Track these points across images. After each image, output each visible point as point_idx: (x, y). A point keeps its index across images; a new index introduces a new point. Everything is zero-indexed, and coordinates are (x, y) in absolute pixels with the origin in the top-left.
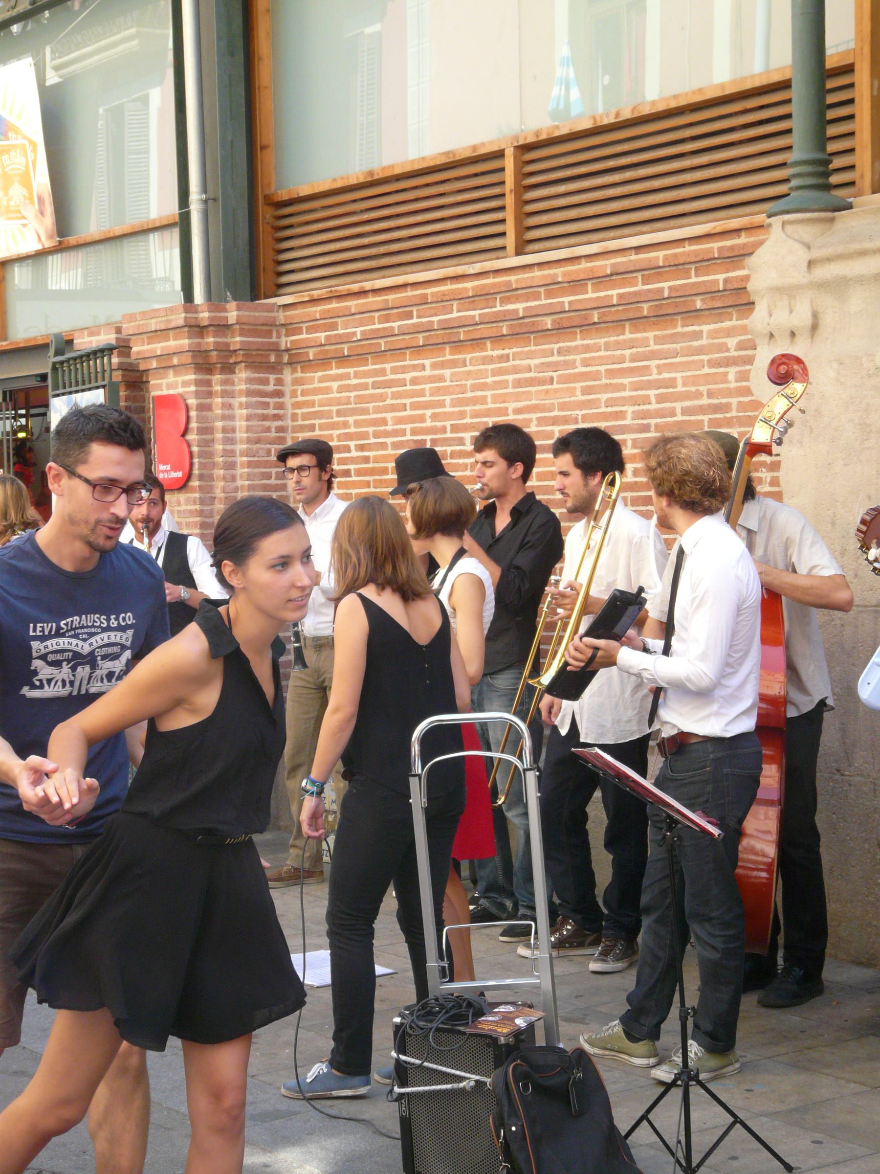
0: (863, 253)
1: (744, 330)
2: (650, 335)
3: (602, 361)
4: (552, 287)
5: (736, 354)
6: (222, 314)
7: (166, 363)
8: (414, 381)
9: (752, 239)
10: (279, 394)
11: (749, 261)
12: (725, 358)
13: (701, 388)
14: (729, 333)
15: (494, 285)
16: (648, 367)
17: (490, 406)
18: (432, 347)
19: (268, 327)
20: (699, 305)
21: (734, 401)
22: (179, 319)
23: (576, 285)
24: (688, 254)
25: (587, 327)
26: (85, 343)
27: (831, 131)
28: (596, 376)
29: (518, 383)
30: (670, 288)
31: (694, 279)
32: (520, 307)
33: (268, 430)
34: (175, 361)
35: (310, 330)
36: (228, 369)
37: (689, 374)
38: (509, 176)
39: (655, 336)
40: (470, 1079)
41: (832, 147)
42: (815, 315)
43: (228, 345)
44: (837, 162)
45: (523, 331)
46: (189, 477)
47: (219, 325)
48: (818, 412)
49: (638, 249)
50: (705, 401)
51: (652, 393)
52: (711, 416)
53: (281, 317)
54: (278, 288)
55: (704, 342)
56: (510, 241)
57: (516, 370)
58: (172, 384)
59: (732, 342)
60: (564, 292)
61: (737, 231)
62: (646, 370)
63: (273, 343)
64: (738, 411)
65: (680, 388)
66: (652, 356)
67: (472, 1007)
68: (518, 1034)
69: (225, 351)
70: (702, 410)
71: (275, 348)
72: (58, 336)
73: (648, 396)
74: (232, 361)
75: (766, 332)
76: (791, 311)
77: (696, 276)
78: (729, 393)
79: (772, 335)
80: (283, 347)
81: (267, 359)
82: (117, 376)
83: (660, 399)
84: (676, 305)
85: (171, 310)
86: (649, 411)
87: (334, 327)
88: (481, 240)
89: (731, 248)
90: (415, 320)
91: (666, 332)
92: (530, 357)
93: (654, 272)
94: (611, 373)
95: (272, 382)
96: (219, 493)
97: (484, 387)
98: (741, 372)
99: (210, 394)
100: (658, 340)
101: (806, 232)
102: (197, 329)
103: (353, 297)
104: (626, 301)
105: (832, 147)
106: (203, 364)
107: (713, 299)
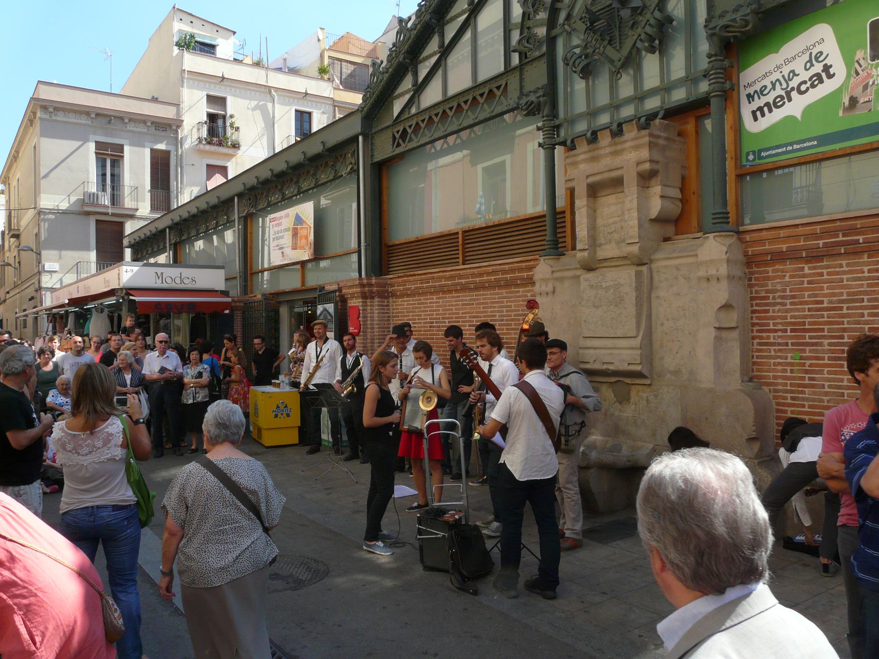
0: (568, 270)
1: (532, 291)
3: (489, 299)
4: (474, 275)
7: (353, 296)
8: (430, 303)
10: (388, 306)
11: (535, 270)
14: (528, 291)
18: (436, 293)
19: (385, 285)
22: (357, 282)
23: (481, 275)
25: (484, 288)
26: (329, 288)
27: (558, 231)
28: (487, 303)
29: (463, 305)
32: (463, 281)
36: (373, 298)
38: (460, 240)
40: (441, 534)
41: (558, 235)
42: (554, 288)
44: (561, 240)
45: (464, 288)
46: (359, 331)
49: (500, 265)
54: (388, 273)
56: (460, 260)
57: (462, 300)
59: (529, 294)
60: (477, 277)
61: (530, 260)
62: (502, 302)
66: (504, 298)
67: (441, 512)
68: (456, 520)
69: (371, 292)
71: (387, 291)
72: (320, 286)
81: (385, 294)
82: (338, 299)
83: (507, 311)
85: (354, 279)
88: (451, 260)
92: (466, 297)
93: (505, 272)
94: (492, 303)
96: (369, 337)
97: (452, 305)
100: (506, 293)
101: (551, 262)
102: (362, 285)
104: (497, 280)
105: (558, 235)
106: (364, 296)
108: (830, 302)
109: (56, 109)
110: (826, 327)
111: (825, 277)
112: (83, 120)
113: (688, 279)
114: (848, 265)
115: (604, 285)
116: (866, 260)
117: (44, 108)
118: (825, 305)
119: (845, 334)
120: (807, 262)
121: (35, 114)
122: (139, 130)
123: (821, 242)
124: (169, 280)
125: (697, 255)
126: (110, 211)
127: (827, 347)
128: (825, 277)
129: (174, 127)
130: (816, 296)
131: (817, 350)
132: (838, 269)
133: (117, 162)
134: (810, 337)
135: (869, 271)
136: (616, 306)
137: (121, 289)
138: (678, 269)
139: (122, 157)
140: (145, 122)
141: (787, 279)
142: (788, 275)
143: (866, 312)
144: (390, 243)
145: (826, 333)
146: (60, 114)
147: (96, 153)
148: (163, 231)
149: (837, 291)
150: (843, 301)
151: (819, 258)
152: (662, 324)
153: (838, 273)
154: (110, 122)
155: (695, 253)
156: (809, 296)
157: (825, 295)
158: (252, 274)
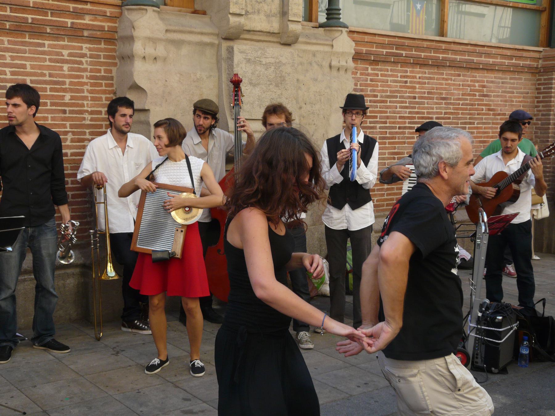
0: (191, 32)
2: (5, 39)
5: (68, 58)
9: (95, 8)
12: (61, 59)
13: (45, 72)
14: (64, 47)
16: (5, 55)
20: (48, 31)
21: (68, 81)
24: (53, 5)
30: (32, 18)
31: (49, 18)
37: (35, 63)
39: (8, 40)
48: (170, 93)
50: (47, 78)
51: (7, 70)
52: (52, 86)
55: (46, 49)
59: (65, 52)
64: (69, 85)
65: (29, 70)
70: (45, 82)
73: (5, 71)
75: (142, 56)
76: (155, 50)
77: (51, 17)
78: (64, 76)
79: (144, 57)
84: (32, 27)
86: (5, 78)
89: (82, 9)
91: (17, 39)
98: (71, 67)
107: (58, 30)
108: (381, 97)
110: (378, 115)
111: (380, 77)
113: (321, 66)
114: (391, 70)
115: (264, 61)
116: (399, 68)
118: (379, 98)
119: (388, 120)
120: (371, 64)
123: (385, 51)
125: (332, 46)
127: (379, 130)
128: (380, 77)
130: (374, 91)
131: (373, 132)
132: (386, 73)
134: (370, 123)
135: (401, 77)
136: (277, 86)
138: (314, 55)
141: (358, 75)
142: (359, 72)
143: (398, 105)
145: (378, 120)
149: (385, 89)
150: (388, 97)
151: (375, 62)
152: (301, 108)
153: (386, 76)
155: (330, 43)
156: (371, 91)
157: (379, 91)
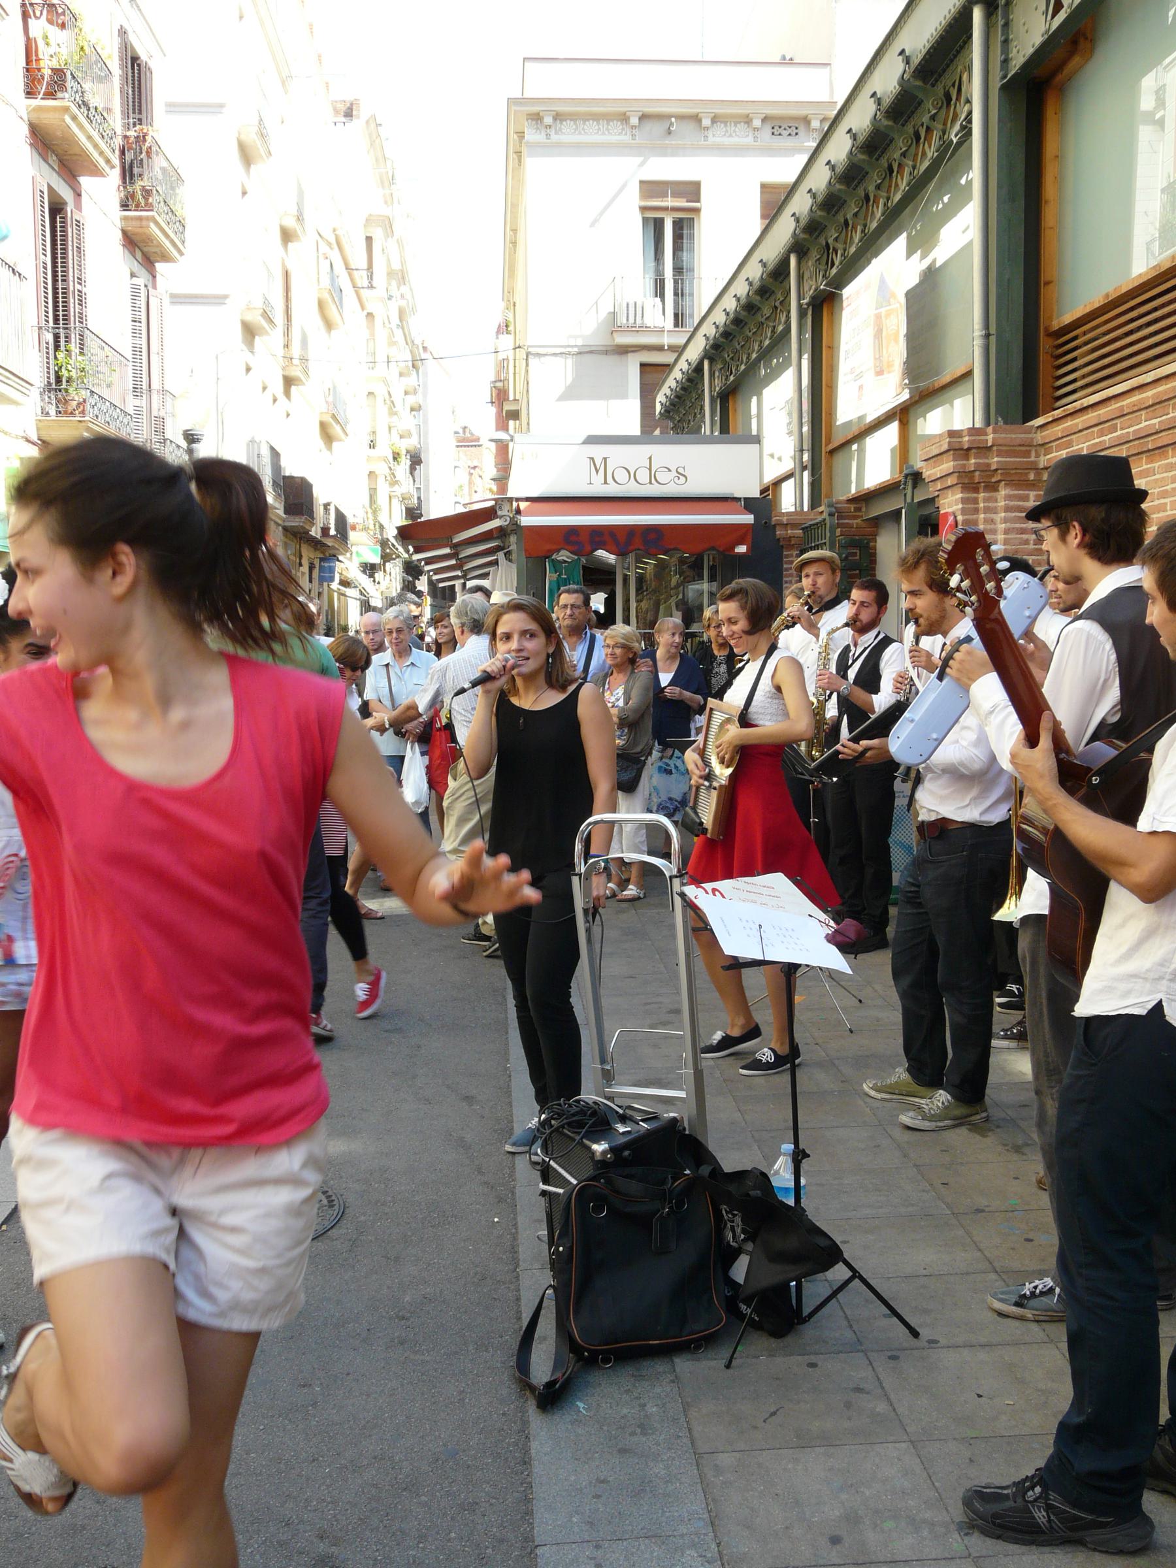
6: (982, 438)
15: (1166, 391)
17: (1169, 513)
19: (1027, 448)
33: (1027, 542)
34: (949, 483)
35: (1059, 449)
36: (993, 487)
43: (989, 465)
47: (979, 448)
53: (1040, 437)
58: (951, 504)
63: (1032, 462)
69: (986, 470)
71: (1034, 467)
74: (993, 480)
80: (1041, 466)
87: (1069, 445)
90: (1119, 433)
95: (1032, 498)
99: (976, 511)
103: (1079, 414)
106: (970, 483)
109: (558, 117)
112: (615, 134)
117: (536, 118)
121: (521, 135)
122: (735, 140)
124: (622, 476)
126: (666, 340)
129: (815, 124)
133: (683, 228)
137: (510, 500)
139: (697, 211)
140: (747, 120)
144: (1056, 325)
146: (568, 126)
147: (643, 209)
148: (699, 369)
154: (669, 132)
158: (832, 452)
